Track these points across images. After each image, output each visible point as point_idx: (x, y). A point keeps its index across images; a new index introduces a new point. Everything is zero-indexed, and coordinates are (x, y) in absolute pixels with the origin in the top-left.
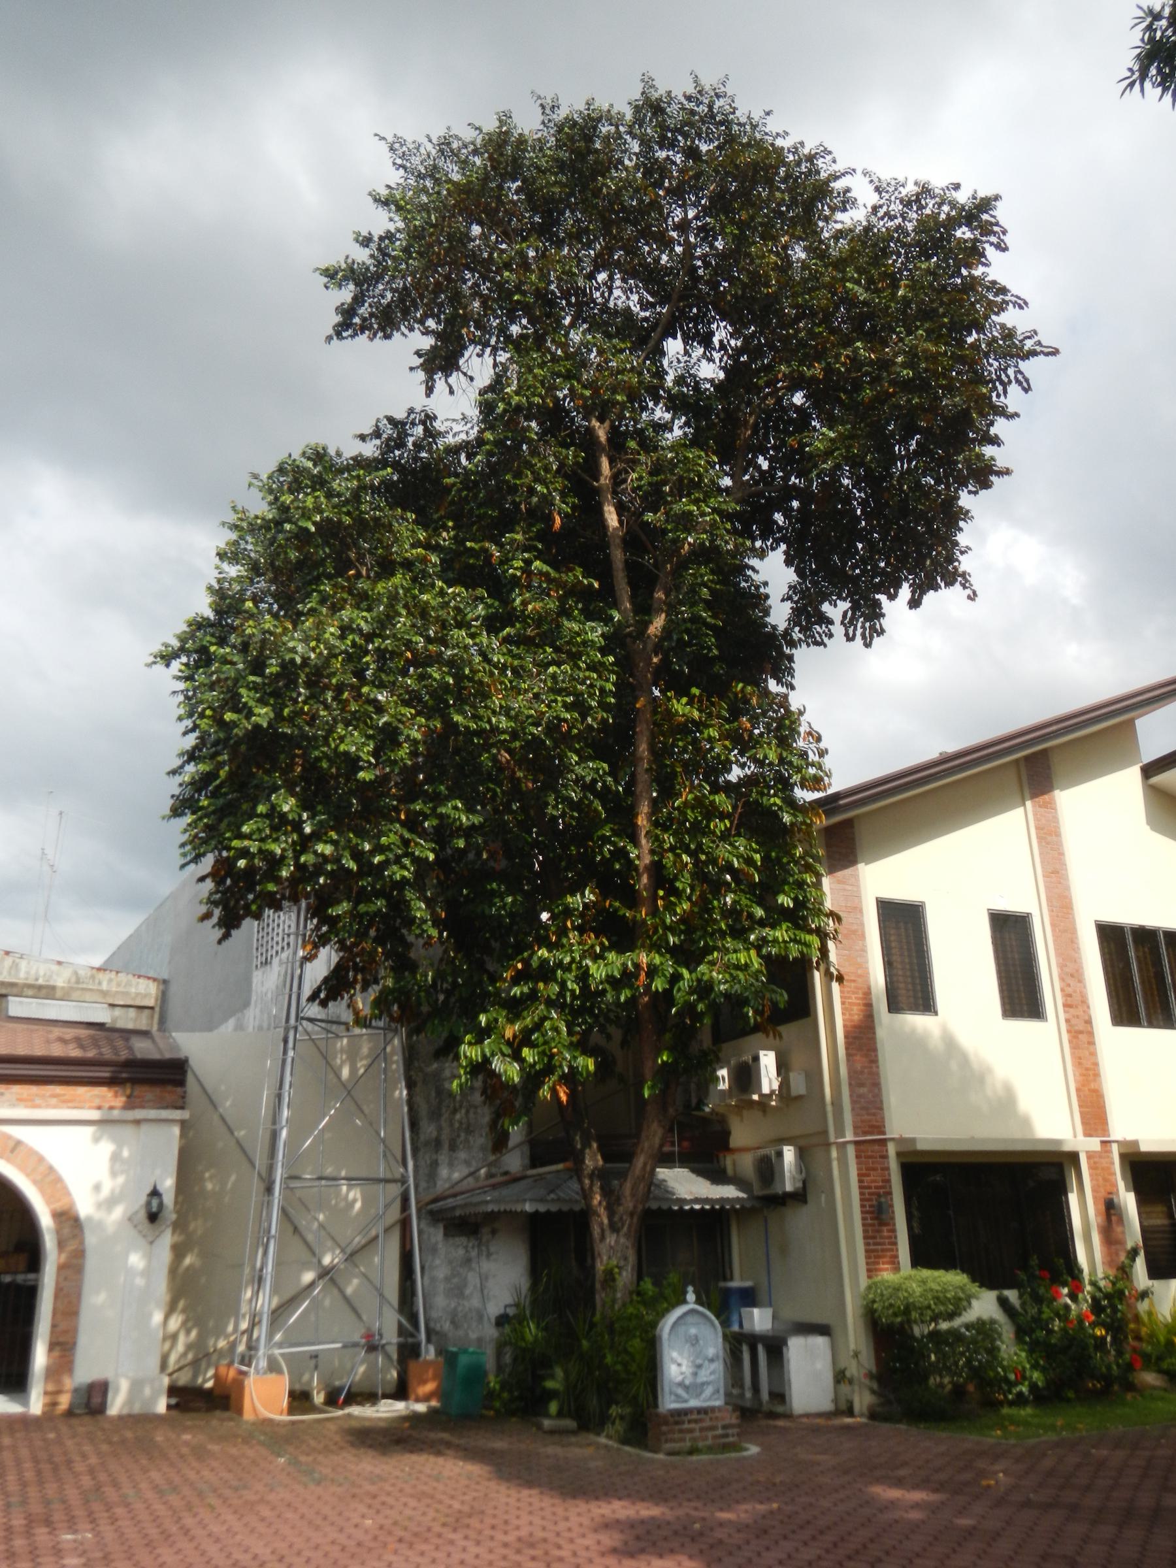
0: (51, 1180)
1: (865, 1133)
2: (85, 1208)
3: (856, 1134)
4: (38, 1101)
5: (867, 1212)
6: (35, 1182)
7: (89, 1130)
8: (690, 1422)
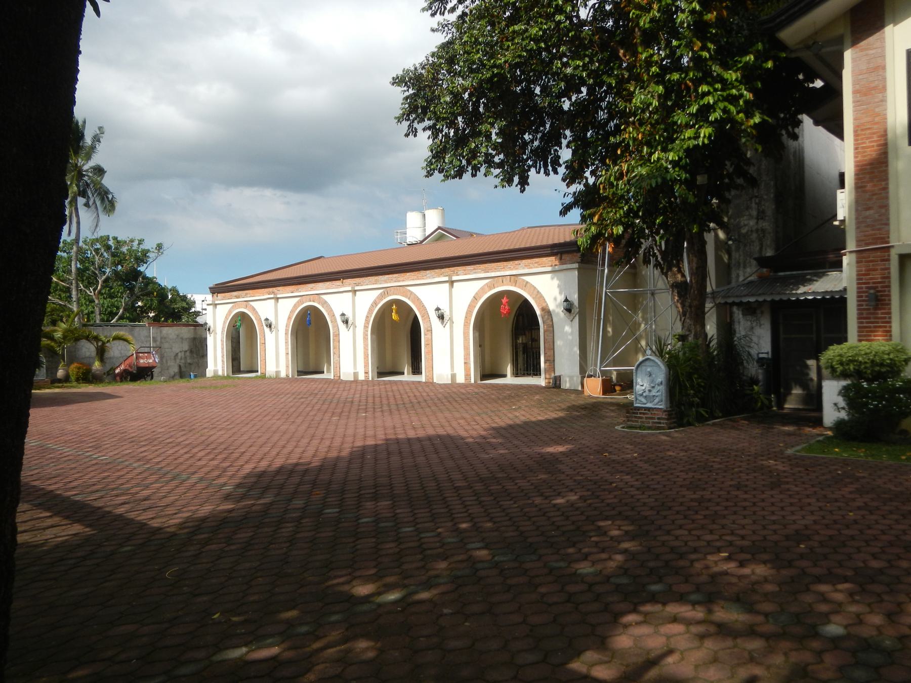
0: (539, 296)
1: (867, 244)
2: (552, 307)
3: (858, 246)
4: (531, 265)
5: (863, 301)
6: (533, 298)
7: (549, 276)
8: (640, 413)
